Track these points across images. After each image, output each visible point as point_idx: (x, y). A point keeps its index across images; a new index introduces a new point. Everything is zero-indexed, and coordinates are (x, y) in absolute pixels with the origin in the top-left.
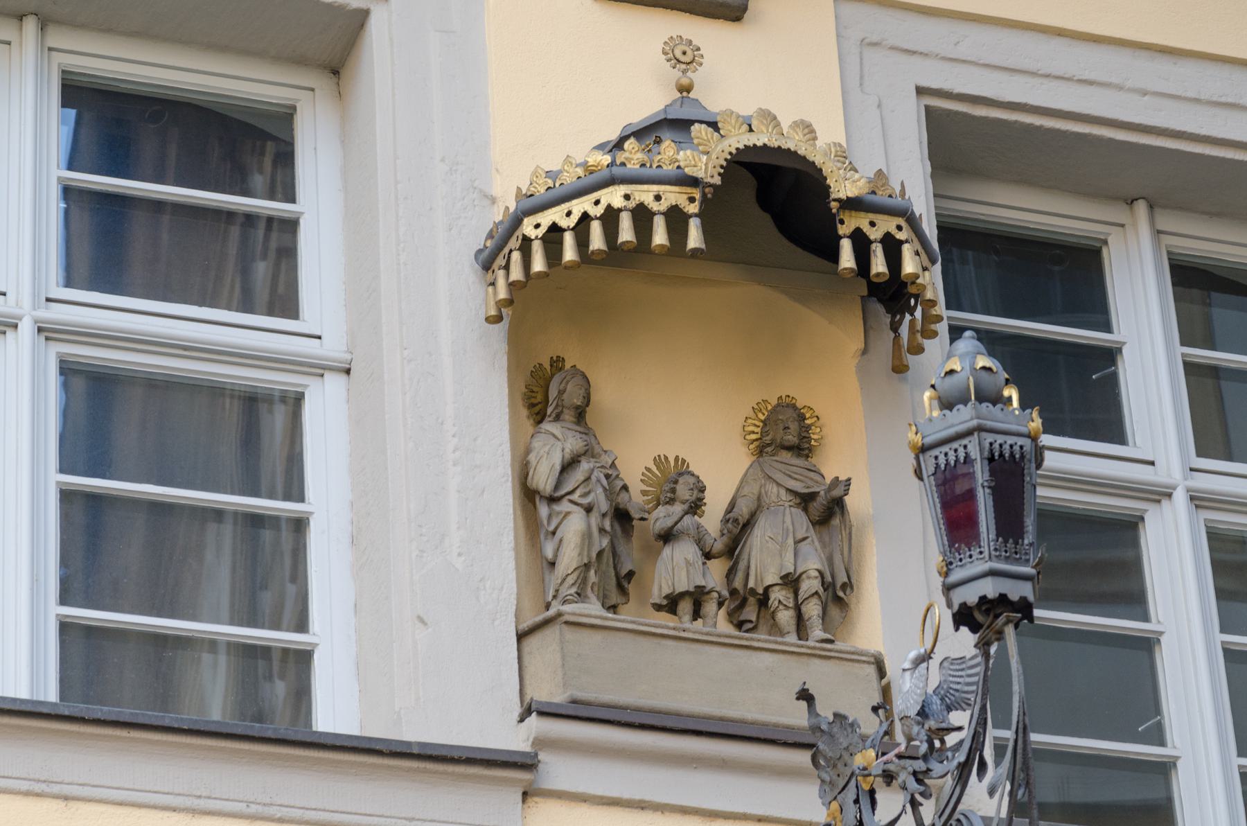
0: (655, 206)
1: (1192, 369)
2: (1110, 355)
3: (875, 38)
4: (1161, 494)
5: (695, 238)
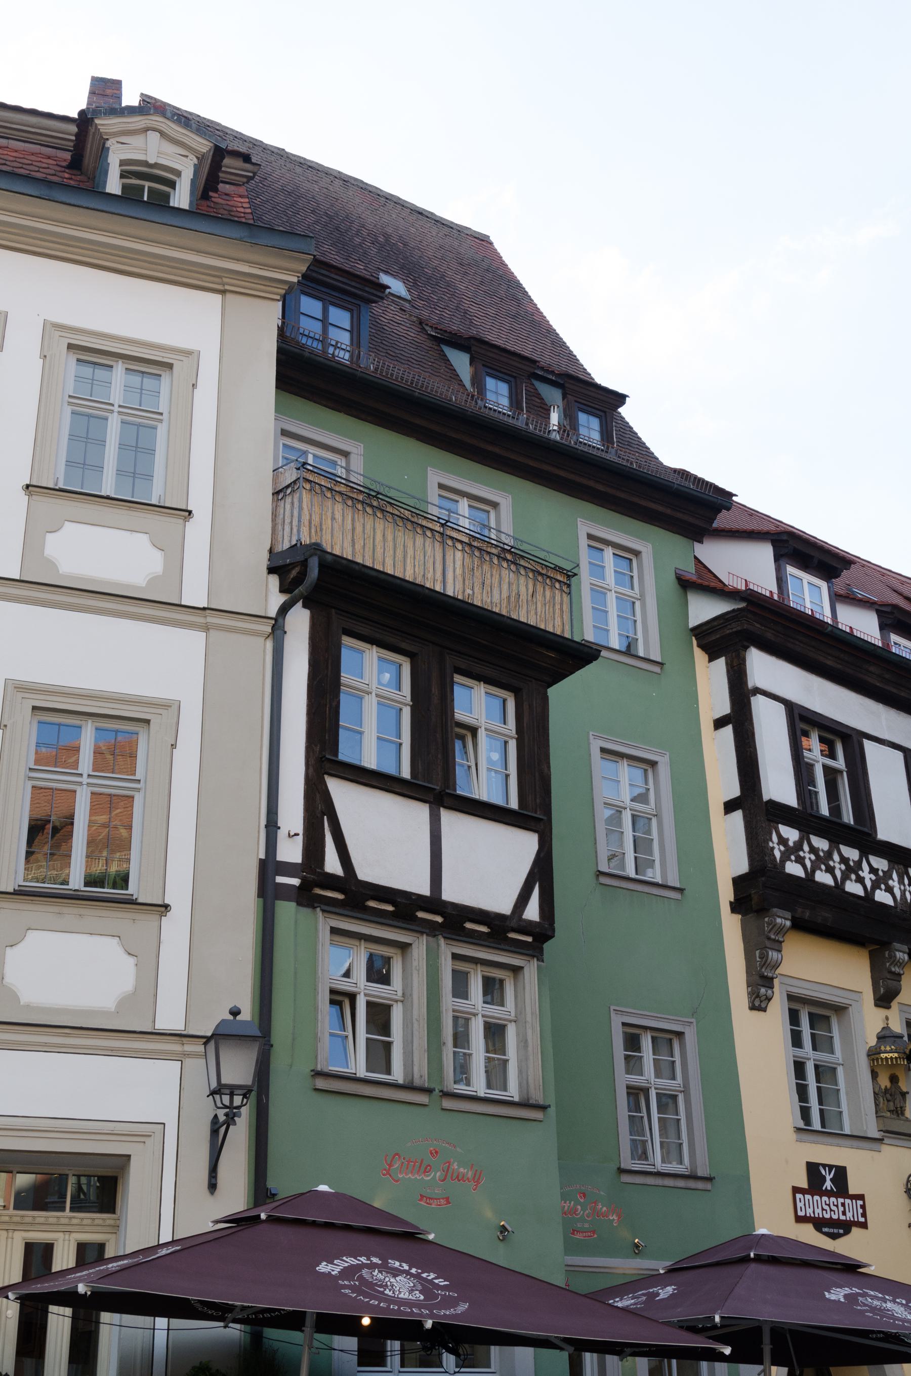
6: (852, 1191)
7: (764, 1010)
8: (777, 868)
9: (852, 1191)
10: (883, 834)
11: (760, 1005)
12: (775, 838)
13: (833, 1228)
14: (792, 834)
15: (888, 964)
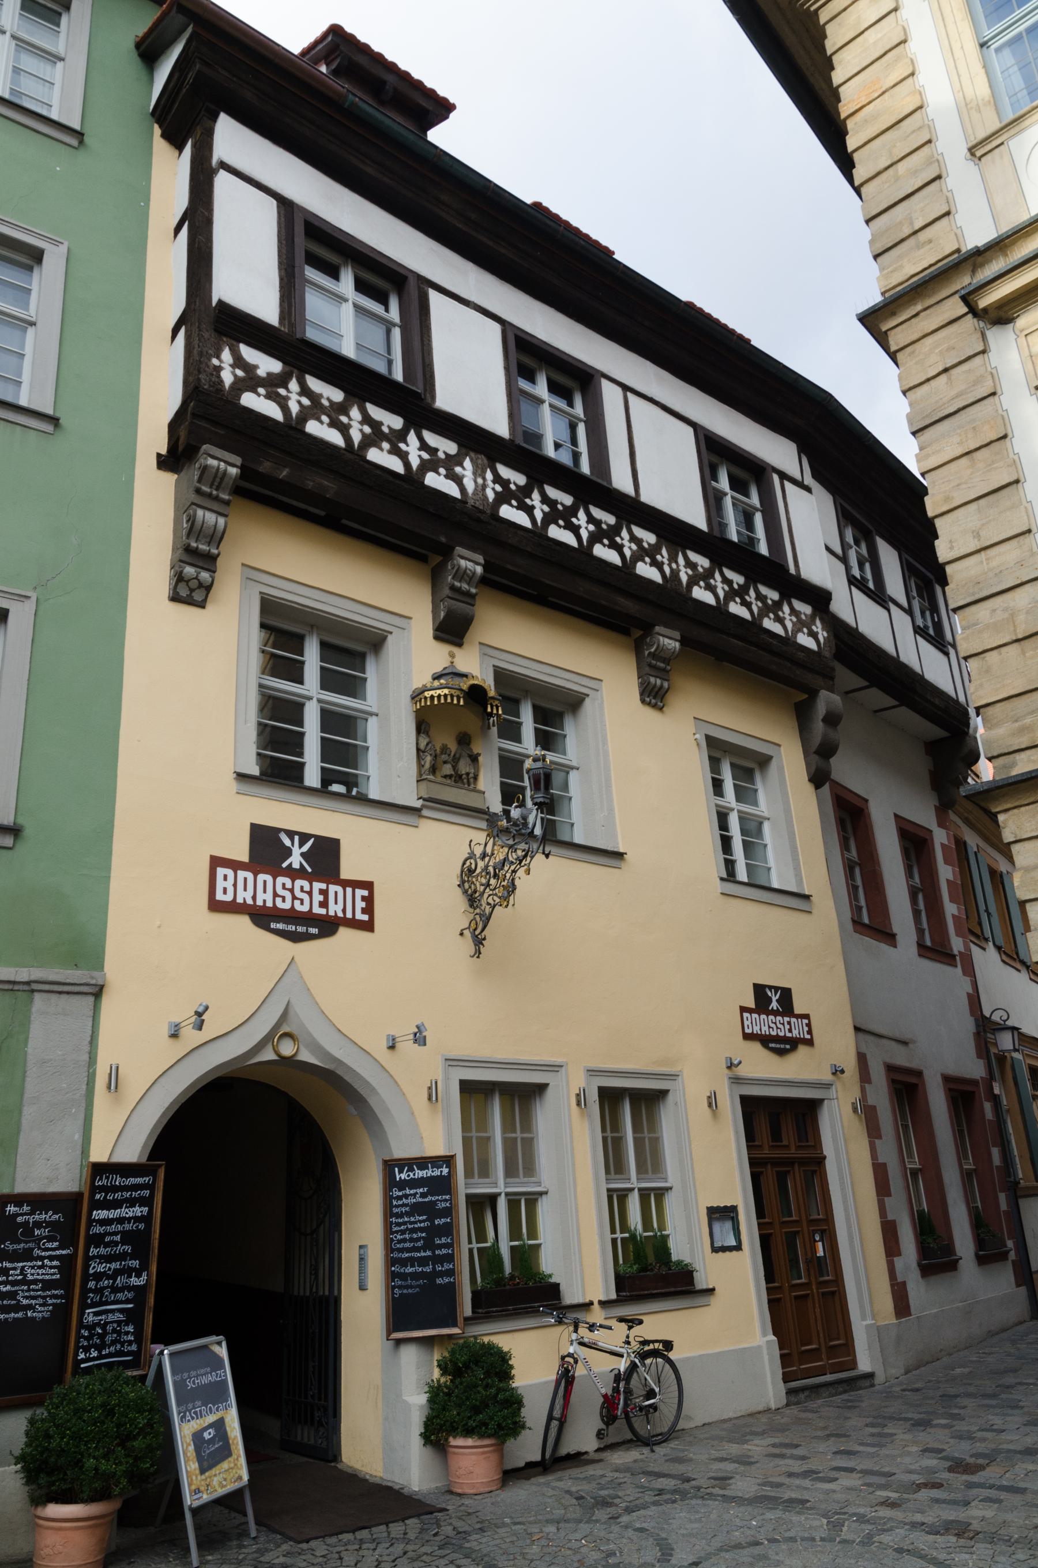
5: (462, 703)
6: (344, 875)
7: (202, 605)
8: (224, 395)
9: (344, 875)
10: (444, 401)
11: (190, 596)
12: (226, 355)
13: (288, 923)
14: (267, 365)
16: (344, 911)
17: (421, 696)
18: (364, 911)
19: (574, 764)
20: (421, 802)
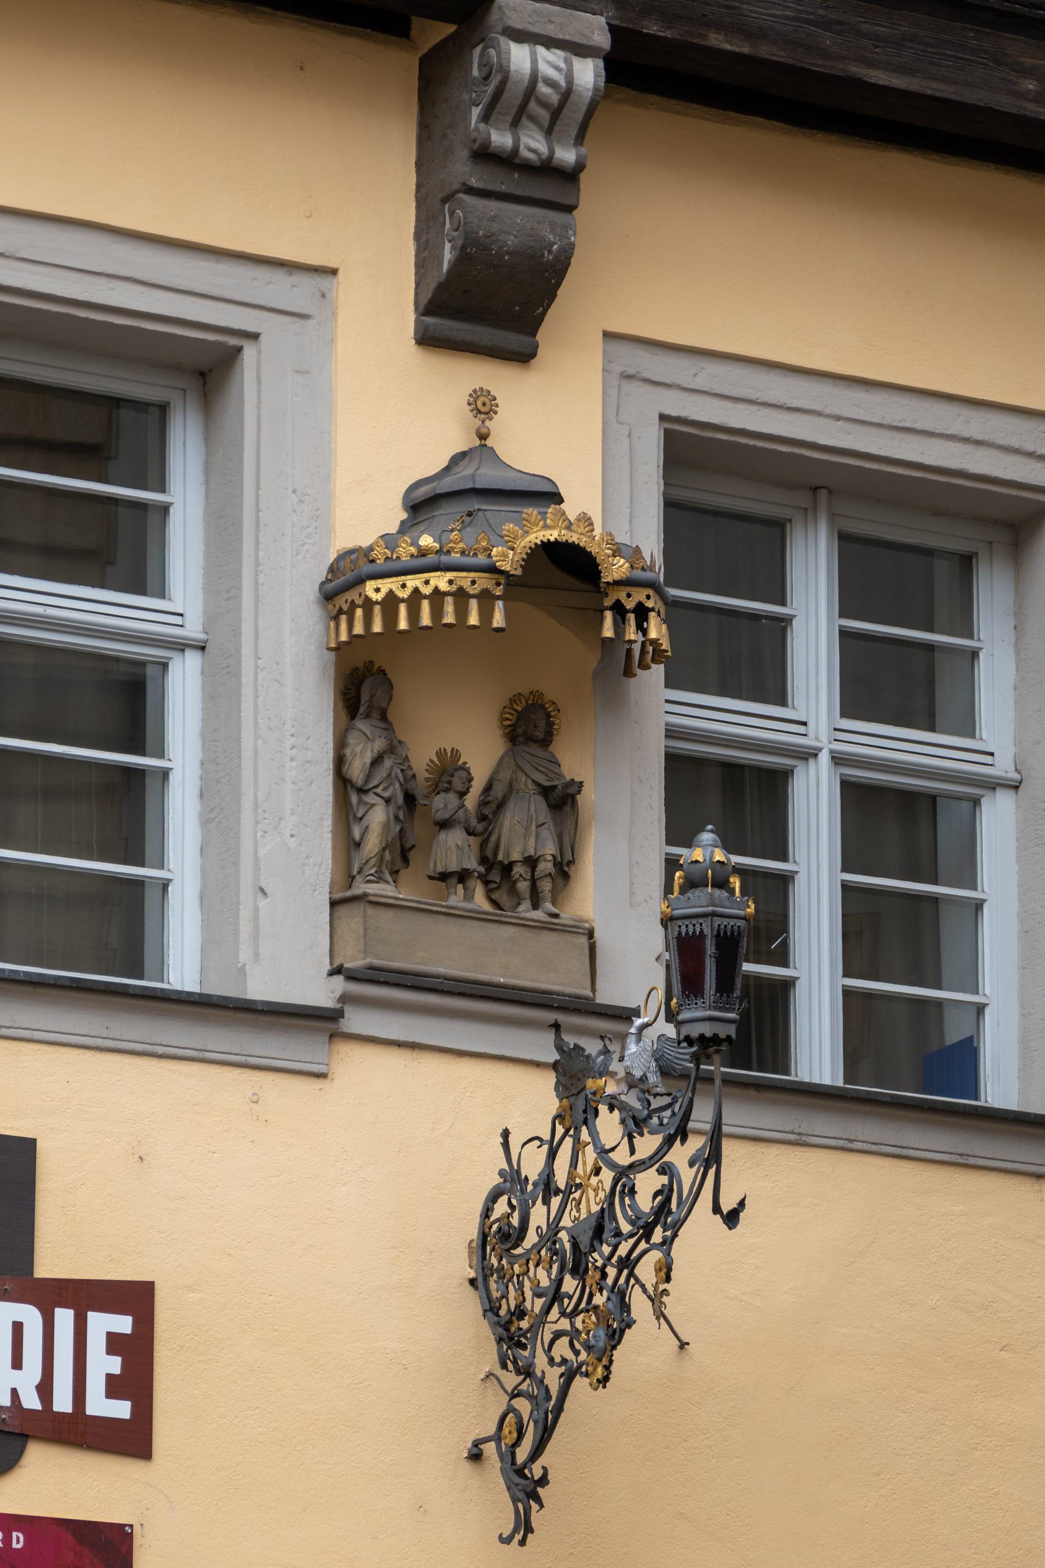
0: (472, 590)
1: (845, 635)
2: (783, 624)
3: (631, 372)
4: (809, 755)
5: (498, 620)
15: (476, 112)
16: (45, 1389)
17: (353, 595)
18: (114, 1388)
19: (1003, 767)
20: (339, 984)
